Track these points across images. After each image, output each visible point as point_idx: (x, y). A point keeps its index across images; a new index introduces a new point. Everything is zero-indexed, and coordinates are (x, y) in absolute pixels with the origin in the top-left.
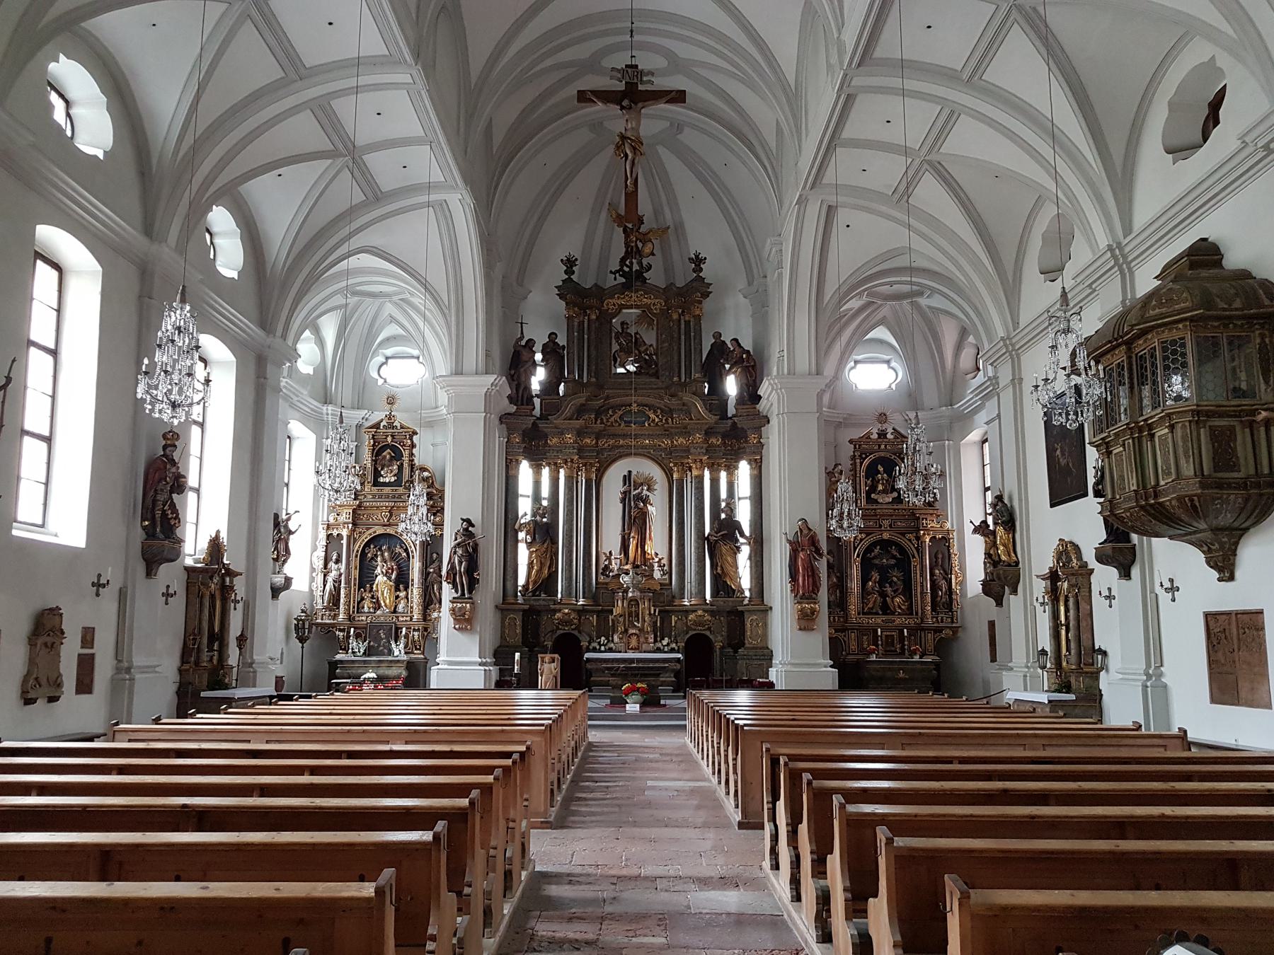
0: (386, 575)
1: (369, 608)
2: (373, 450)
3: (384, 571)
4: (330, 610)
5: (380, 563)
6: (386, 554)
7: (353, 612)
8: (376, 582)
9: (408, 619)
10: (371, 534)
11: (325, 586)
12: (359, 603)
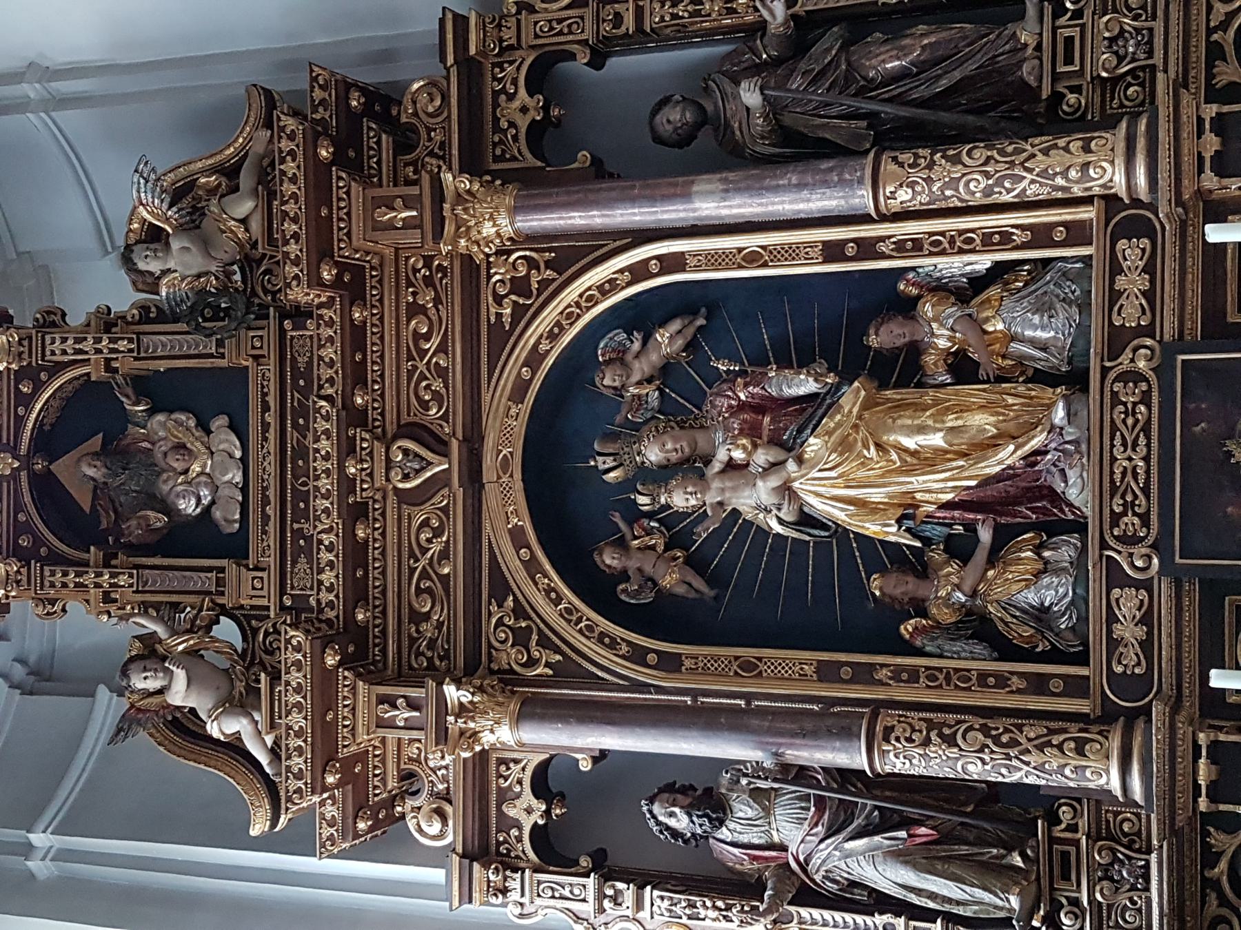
0: (791, 448)
1: (1046, 568)
2: (56, 559)
3: (762, 457)
4: (1065, 868)
5: (712, 498)
6: (653, 454)
7: (1077, 687)
8: (840, 514)
9: (1132, 252)
10: (532, 567)
11: (880, 902)
12: (1006, 650)
